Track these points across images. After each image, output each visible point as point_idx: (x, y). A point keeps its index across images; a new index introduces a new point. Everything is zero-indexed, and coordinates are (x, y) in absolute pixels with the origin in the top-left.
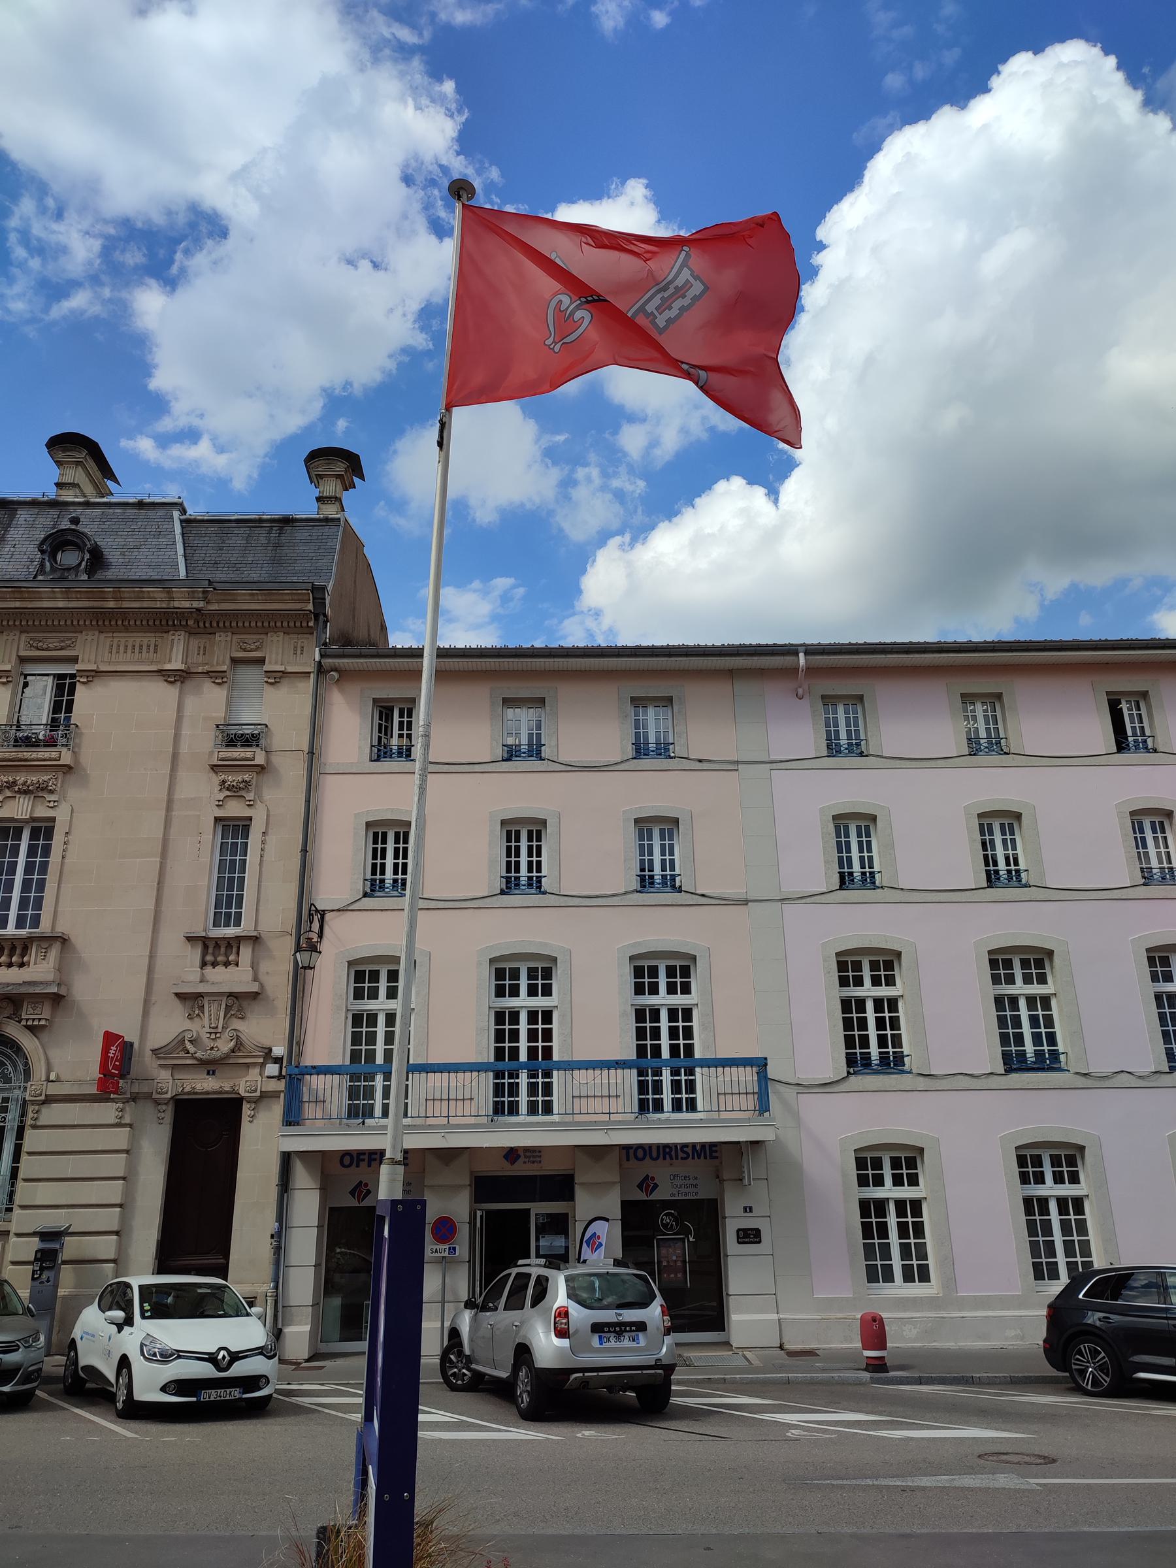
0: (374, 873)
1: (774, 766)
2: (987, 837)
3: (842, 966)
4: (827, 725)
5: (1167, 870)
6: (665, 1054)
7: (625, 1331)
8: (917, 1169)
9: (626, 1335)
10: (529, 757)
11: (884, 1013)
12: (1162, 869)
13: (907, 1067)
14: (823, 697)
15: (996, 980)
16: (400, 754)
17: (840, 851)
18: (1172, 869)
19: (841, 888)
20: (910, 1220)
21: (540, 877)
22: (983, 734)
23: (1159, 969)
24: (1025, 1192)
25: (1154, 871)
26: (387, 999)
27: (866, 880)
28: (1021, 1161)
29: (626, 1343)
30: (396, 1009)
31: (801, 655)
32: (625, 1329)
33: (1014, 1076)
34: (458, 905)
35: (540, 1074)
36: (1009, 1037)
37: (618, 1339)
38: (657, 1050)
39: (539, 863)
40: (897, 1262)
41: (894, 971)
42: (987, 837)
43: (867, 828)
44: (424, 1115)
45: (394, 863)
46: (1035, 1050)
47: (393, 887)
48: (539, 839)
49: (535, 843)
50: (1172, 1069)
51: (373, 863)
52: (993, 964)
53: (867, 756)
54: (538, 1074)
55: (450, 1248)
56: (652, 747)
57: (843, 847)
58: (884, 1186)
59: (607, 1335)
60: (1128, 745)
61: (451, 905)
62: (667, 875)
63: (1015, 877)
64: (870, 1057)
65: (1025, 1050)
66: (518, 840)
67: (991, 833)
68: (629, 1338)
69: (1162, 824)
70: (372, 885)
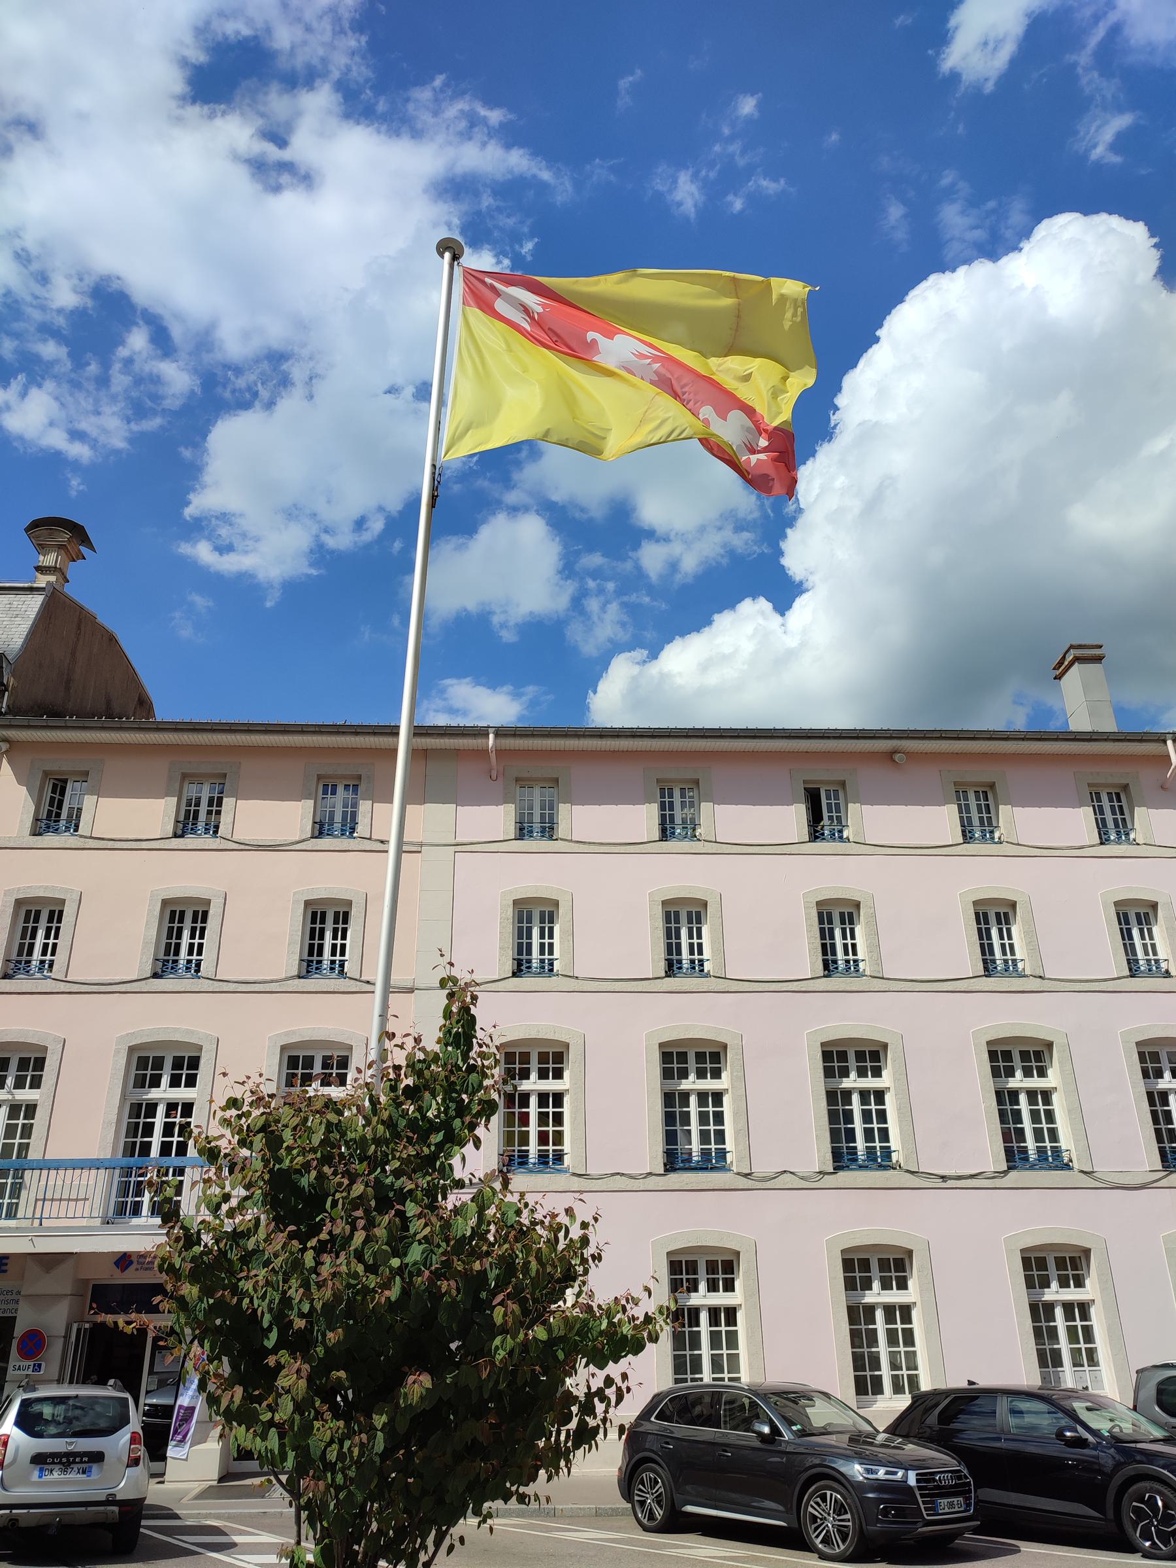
0: (311, 953)
1: (459, 848)
2: (983, 926)
3: (827, 1056)
4: (662, 807)
5: (1153, 962)
6: (155, 1151)
7: (74, 1462)
8: (733, 1274)
9: (76, 1467)
10: (205, 834)
11: (871, 1105)
12: (1006, 961)
13: (565, 1165)
14: (517, 780)
15: (996, 1072)
16: (207, 830)
17: (823, 937)
18: (855, 961)
19: (514, 975)
20: (899, 1326)
21: (344, 961)
22: (976, 822)
23: (1150, 1065)
24: (851, 1298)
25: (1141, 962)
26: (14, 1089)
27: (850, 968)
28: (848, 1265)
29: (73, 1476)
30: (37, 1100)
31: (491, 736)
32: (68, 1460)
33: (673, 1177)
34: (103, 989)
35: (134, 1172)
36: (1012, 1136)
37: (64, 1471)
38: (146, 1149)
39: (551, 945)
40: (885, 1372)
41: (720, 1063)
42: (983, 926)
43: (698, 914)
44: (31, 1216)
45: (333, 944)
46: (702, 1149)
47: (187, 968)
48: (346, 921)
49: (341, 926)
50: (837, 1169)
51: (310, 944)
52: (993, 1055)
53: (557, 840)
54: (131, 1172)
55: (34, 1365)
56: (337, 826)
57: (826, 934)
58: (871, 1290)
59: (50, 1467)
60: (823, 834)
61: (95, 989)
62: (544, 959)
63: (1011, 969)
64: (528, 1156)
65: (725, 1149)
66: (323, 921)
67: (677, 921)
68: (79, 1470)
69: (1006, 914)
70: (164, 965)
